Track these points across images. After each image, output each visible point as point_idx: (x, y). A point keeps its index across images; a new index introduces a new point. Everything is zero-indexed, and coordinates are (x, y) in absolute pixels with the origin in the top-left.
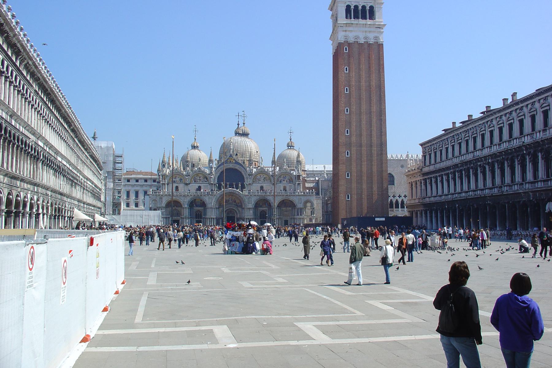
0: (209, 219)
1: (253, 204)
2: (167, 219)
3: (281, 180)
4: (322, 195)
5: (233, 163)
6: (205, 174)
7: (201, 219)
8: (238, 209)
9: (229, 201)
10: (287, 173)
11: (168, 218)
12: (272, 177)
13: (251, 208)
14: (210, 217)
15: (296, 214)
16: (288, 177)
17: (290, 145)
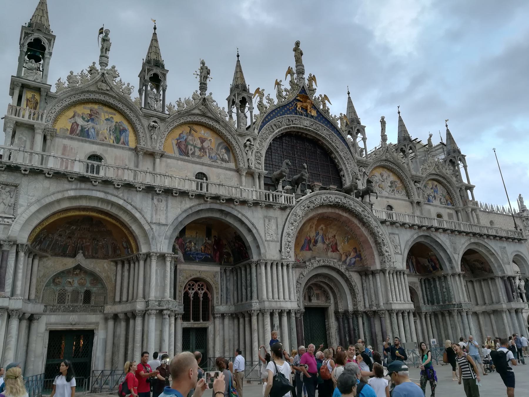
3: (428, 196)
6: (224, 131)
9: (316, 242)
12: (412, 183)
13: (404, 274)
14: (274, 305)
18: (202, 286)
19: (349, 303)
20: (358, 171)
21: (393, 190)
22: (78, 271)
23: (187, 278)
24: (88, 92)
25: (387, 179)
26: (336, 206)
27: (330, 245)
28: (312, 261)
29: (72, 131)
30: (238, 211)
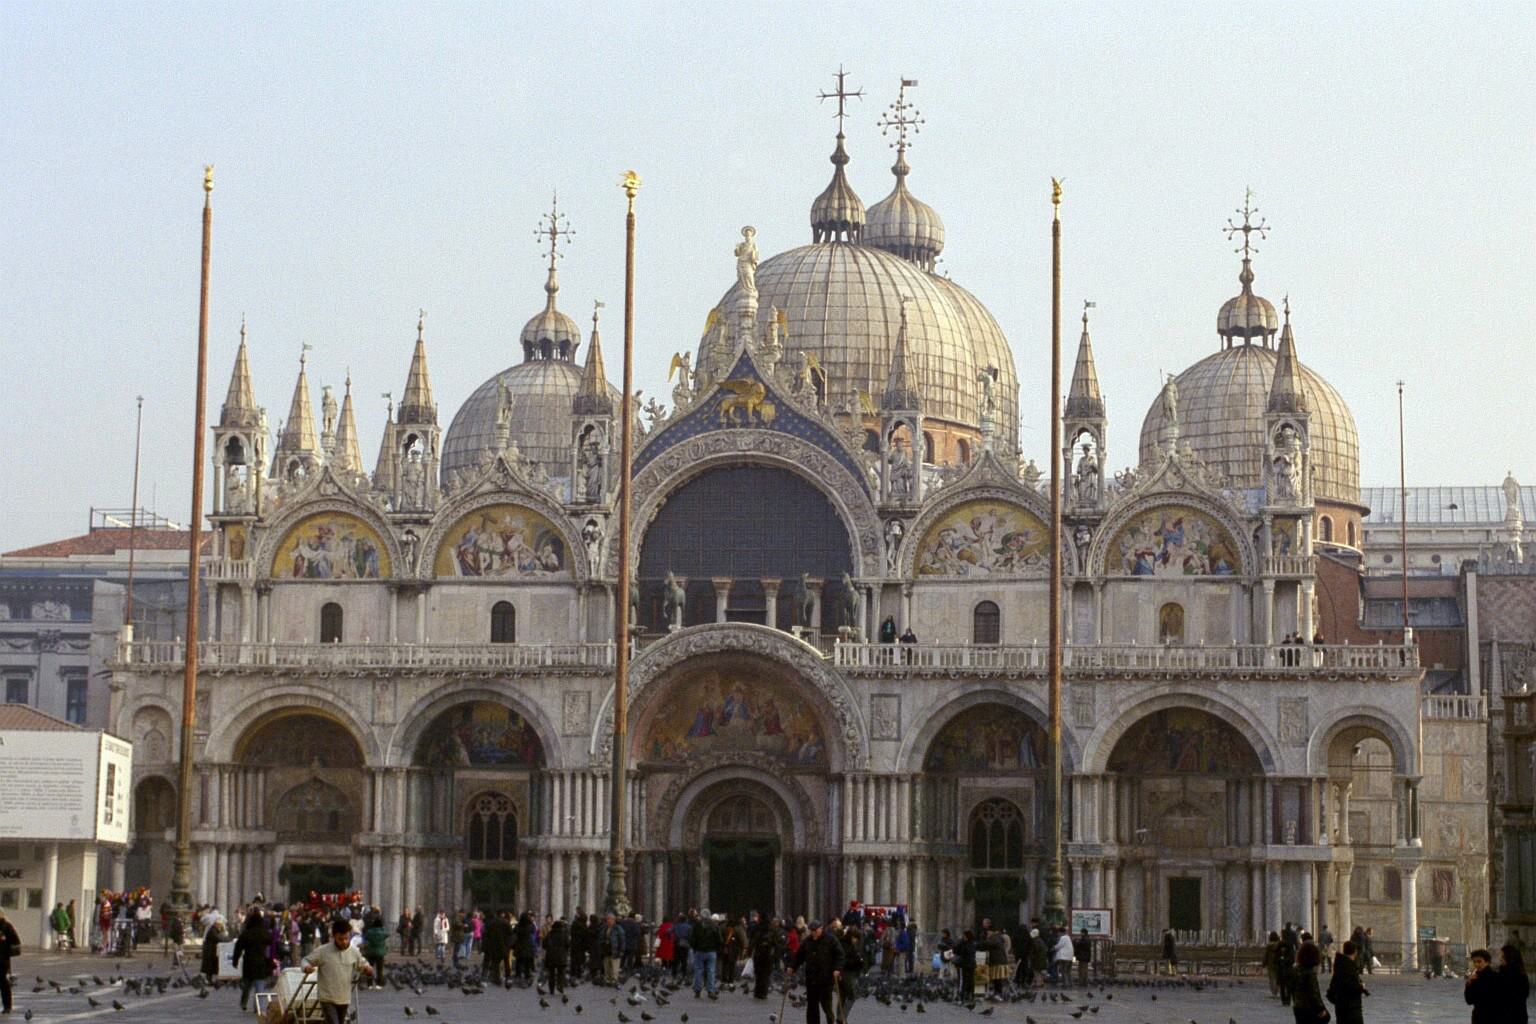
0: (566, 857)
1: (915, 749)
2: (249, 858)
3: (1140, 556)
4: (1486, 682)
5: (761, 423)
6: (544, 512)
7: (512, 865)
8: (795, 788)
9: (725, 718)
10: (1192, 496)
11: (263, 849)
13: (899, 781)
14: (567, 844)
15: (1262, 823)
16: (1193, 533)
17: (1242, 323)
18: (506, 803)
19: (796, 835)
20: (880, 534)
21: (1012, 559)
22: (318, 785)
23: (471, 793)
24: (309, 504)
25: (991, 532)
26: (730, 651)
27: (762, 721)
28: (703, 758)
29: (296, 572)
30: (514, 689)
